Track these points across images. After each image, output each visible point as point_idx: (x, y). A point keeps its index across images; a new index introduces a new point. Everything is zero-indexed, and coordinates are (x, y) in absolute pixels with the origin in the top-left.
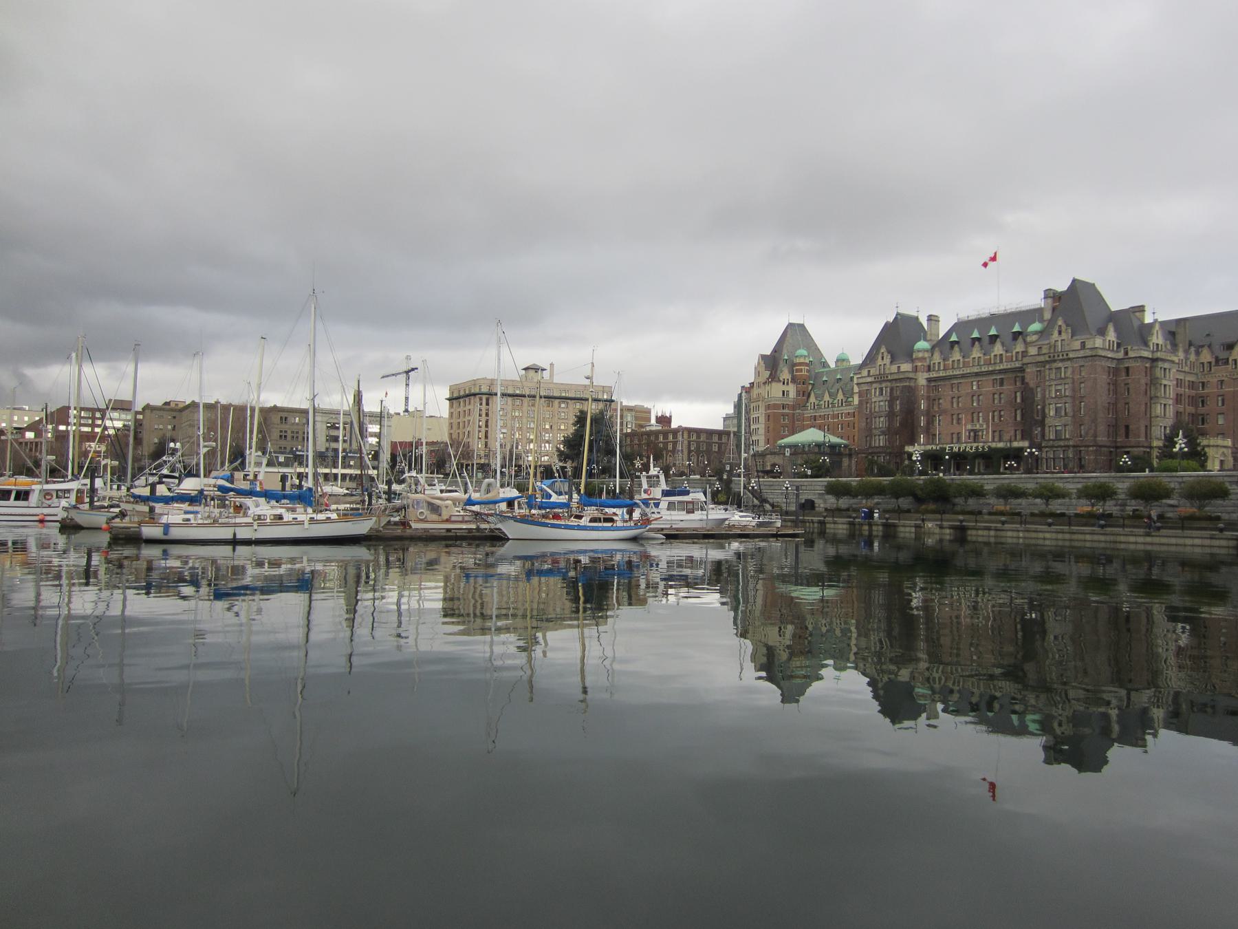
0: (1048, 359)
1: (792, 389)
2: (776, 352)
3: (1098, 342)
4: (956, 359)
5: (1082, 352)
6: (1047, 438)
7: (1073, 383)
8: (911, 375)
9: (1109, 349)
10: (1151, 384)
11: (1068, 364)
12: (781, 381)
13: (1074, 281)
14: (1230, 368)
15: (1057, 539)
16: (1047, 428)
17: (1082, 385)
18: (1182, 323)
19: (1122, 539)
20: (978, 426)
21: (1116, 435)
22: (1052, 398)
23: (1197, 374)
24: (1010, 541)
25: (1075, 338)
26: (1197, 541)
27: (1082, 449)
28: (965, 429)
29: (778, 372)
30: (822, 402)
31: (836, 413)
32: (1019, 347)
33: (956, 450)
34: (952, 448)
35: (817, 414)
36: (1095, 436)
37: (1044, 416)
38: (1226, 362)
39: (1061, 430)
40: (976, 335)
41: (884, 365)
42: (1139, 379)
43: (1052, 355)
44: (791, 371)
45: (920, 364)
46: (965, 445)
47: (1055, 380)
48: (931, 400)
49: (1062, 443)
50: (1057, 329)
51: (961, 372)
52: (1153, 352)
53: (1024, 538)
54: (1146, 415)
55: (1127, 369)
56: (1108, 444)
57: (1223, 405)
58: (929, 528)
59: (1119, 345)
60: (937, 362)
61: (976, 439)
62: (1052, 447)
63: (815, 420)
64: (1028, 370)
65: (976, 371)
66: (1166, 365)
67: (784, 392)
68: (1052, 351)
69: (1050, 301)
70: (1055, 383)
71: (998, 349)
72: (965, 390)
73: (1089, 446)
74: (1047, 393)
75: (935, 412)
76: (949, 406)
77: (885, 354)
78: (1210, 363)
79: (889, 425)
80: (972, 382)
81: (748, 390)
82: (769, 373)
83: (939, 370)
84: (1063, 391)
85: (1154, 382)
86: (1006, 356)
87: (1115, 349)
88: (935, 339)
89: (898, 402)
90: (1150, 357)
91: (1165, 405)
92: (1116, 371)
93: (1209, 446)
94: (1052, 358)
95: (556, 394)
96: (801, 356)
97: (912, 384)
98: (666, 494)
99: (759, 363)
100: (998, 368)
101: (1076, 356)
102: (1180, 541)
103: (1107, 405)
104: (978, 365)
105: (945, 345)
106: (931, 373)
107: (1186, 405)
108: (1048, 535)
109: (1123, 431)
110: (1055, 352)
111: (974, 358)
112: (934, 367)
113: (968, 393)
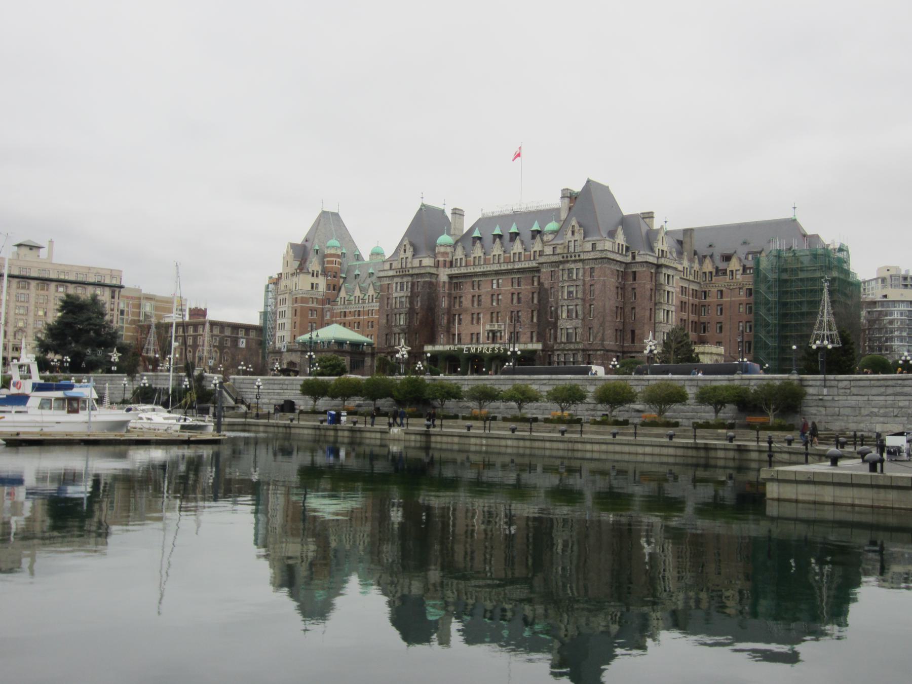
0: (561, 259)
1: (322, 282)
2: (307, 241)
3: (608, 245)
4: (477, 255)
5: (592, 254)
6: (559, 341)
7: (584, 285)
8: (433, 271)
9: (618, 253)
10: (656, 289)
11: (580, 265)
12: (309, 273)
13: (589, 181)
14: (728, 280)
15: (518, 447)
16: (559, 331)
17: (592, 288)
18: (689, 233)
19: (579, 446)
20: (496, 326)
21: (623, 340)
22: (565, 299)
23: (699, 283)
24: (473, 448)
25: (587, 239)
26: (648, 450)
27: (591, 352)
28: (484, 327)
29: (308, 263)
30: (352, 298)
31: (366, 309)
32: (537, 246)
33: (473, 351)
34: (469, 349)
35: (347, 310)
36: (603, 340)
37: (557, 319)
38: (724, 272)
39: (571, 333)
40: (497, 231)
41: (407, 258)
42: (645, 284)
43: (565, 255)
44: (322, 263)
46: (482, 346)
47: (567, 281)
49: (572, 347)
50: (571, 229)
51: (482, 270)
52: (658, 258)
53: (487, 445)
54: (650, 320)
55: (634, 273)
56: (616, 348)
57: (721, 314)
58: (395, 434)
59: (627, 249)
60: (459, 258)
61: (494, 340)
62: (563, 350)
63: (345, 316)
64: (543, 270)
65: (496, 269)
66: (670, 272)
67: (312, 284)
68: (566, 251)
69: (567, 200)
70: (568, 284)
71: (517, 247)
72: (485, 289)
73: (597, 350)
74: (560, 294)
75: (456, 310)
76: (470, 305)
77: (408, 246)
78: (711, 273)
79: (409, 323)
80: (492, 280)
81: (276, 281)
82: (297, 263)
83: (461, 266)
84: (575, 292)
85: (657, 288)
86: (525, 255)
87: (624, 252)
88: (460, 234)
89: (419, 299)
90: (656, 262)
91: (668, 311)
92: (624, 275)
93: (703, 353)
94: (565, 259)
95: (53, 276)
96: (333, 247)
97: (434, 280)
98: (37, 388)
99: (288, 252)
100: (516, 267)
101: (587, 258)
102: (633, 449)
103: (615, 309)
104: (499, 263)
105: (470, 240)
106: (453, 269)
107: (690, 314)
108: (509, 443)
109: (629, 336)
110: (568, 253)
111: (494, 256)
112: (456, 263)
113: (488, 292)
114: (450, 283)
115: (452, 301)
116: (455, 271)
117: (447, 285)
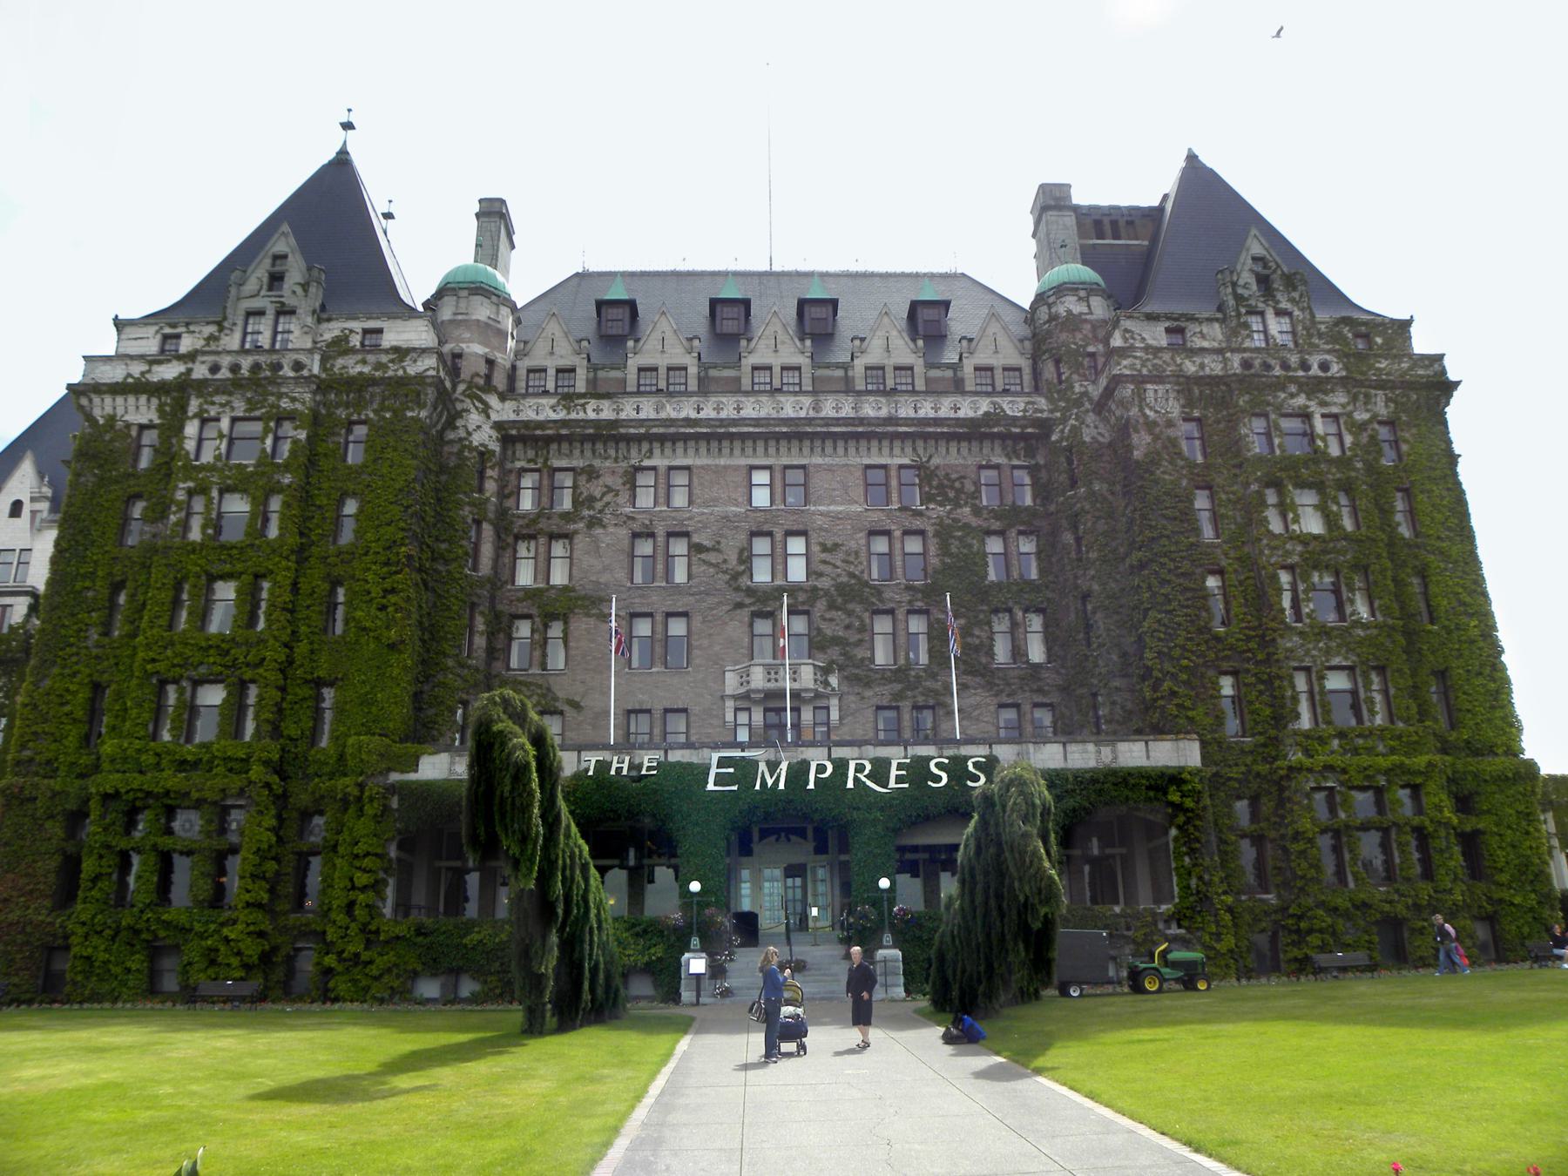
34: (746, 769)
45: (478, 349)
60: (551, 364)
69: (1070, 220)
86: (928, 381)
100: (905, 412)
116: (541, 410)
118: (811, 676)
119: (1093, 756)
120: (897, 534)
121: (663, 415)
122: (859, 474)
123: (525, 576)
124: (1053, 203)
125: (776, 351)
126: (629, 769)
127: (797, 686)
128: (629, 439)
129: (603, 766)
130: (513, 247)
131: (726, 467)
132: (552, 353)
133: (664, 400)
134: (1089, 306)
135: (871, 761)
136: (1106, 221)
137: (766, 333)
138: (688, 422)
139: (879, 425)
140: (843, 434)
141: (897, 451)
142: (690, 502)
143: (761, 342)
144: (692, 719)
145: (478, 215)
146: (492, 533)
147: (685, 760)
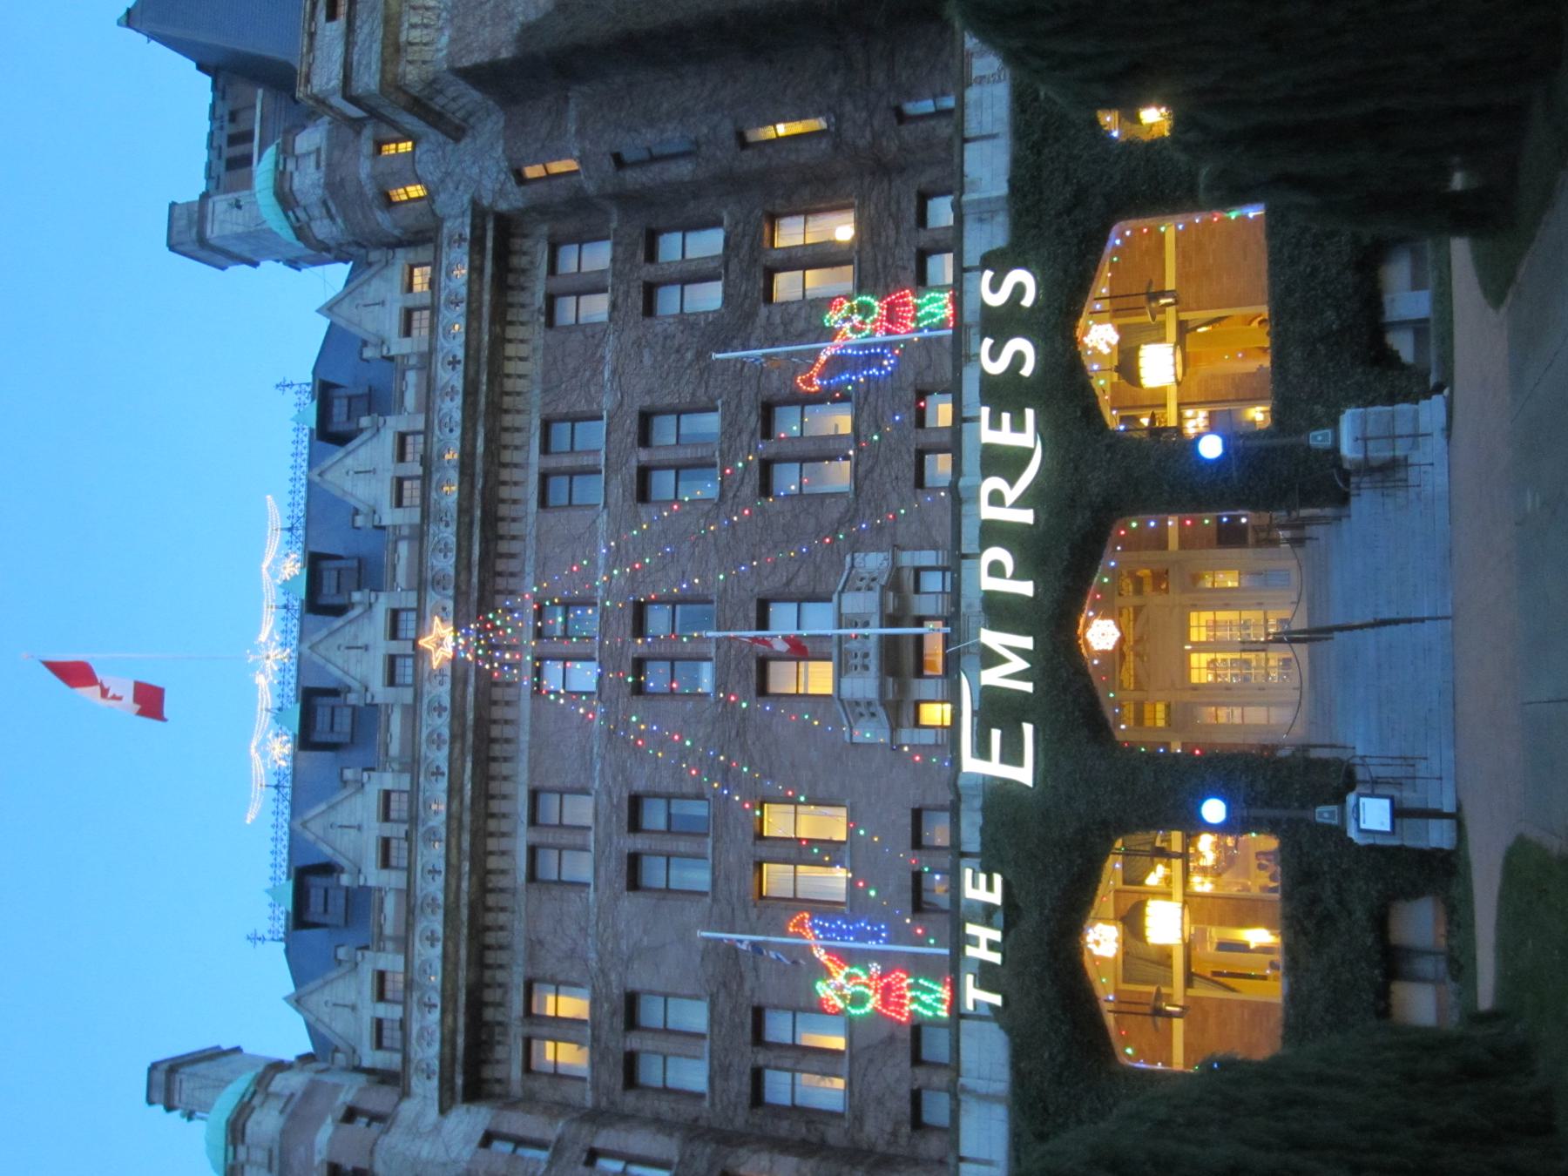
45: (325, 1134)
48: (630, 1101)
51: (440, 757)
60: (371, 1010)
69: (220, 203)
114: (507, 1102)
115: (650, 1105)
117: (518, 1122)
118: (861, 596)
119: (988, 89)
120: (644, 455)
121: (443, 832)
122: (551, 518)
123: (693, 1075)
124: (194, 231)
125: (366, 648)
126: (988, 922)
127: (875, 620)
128: (483, 888)
129: (987, 976)
130: (237, 1050)
131: (534, 732)
132: (353, 1008)
133: (421, 830)
134: (309, 154)
135: (985, 476)
136: (228, 152)
137: (340, 662)
138: (453, 791)
139: (473, 486)
140: (485, 541)
141: (517, 457)
142: (584, 791)
143: (353, 672)
144: (929, 801)
145: (170, 1108)
146: (612, 1133)
147: (978, 819)
